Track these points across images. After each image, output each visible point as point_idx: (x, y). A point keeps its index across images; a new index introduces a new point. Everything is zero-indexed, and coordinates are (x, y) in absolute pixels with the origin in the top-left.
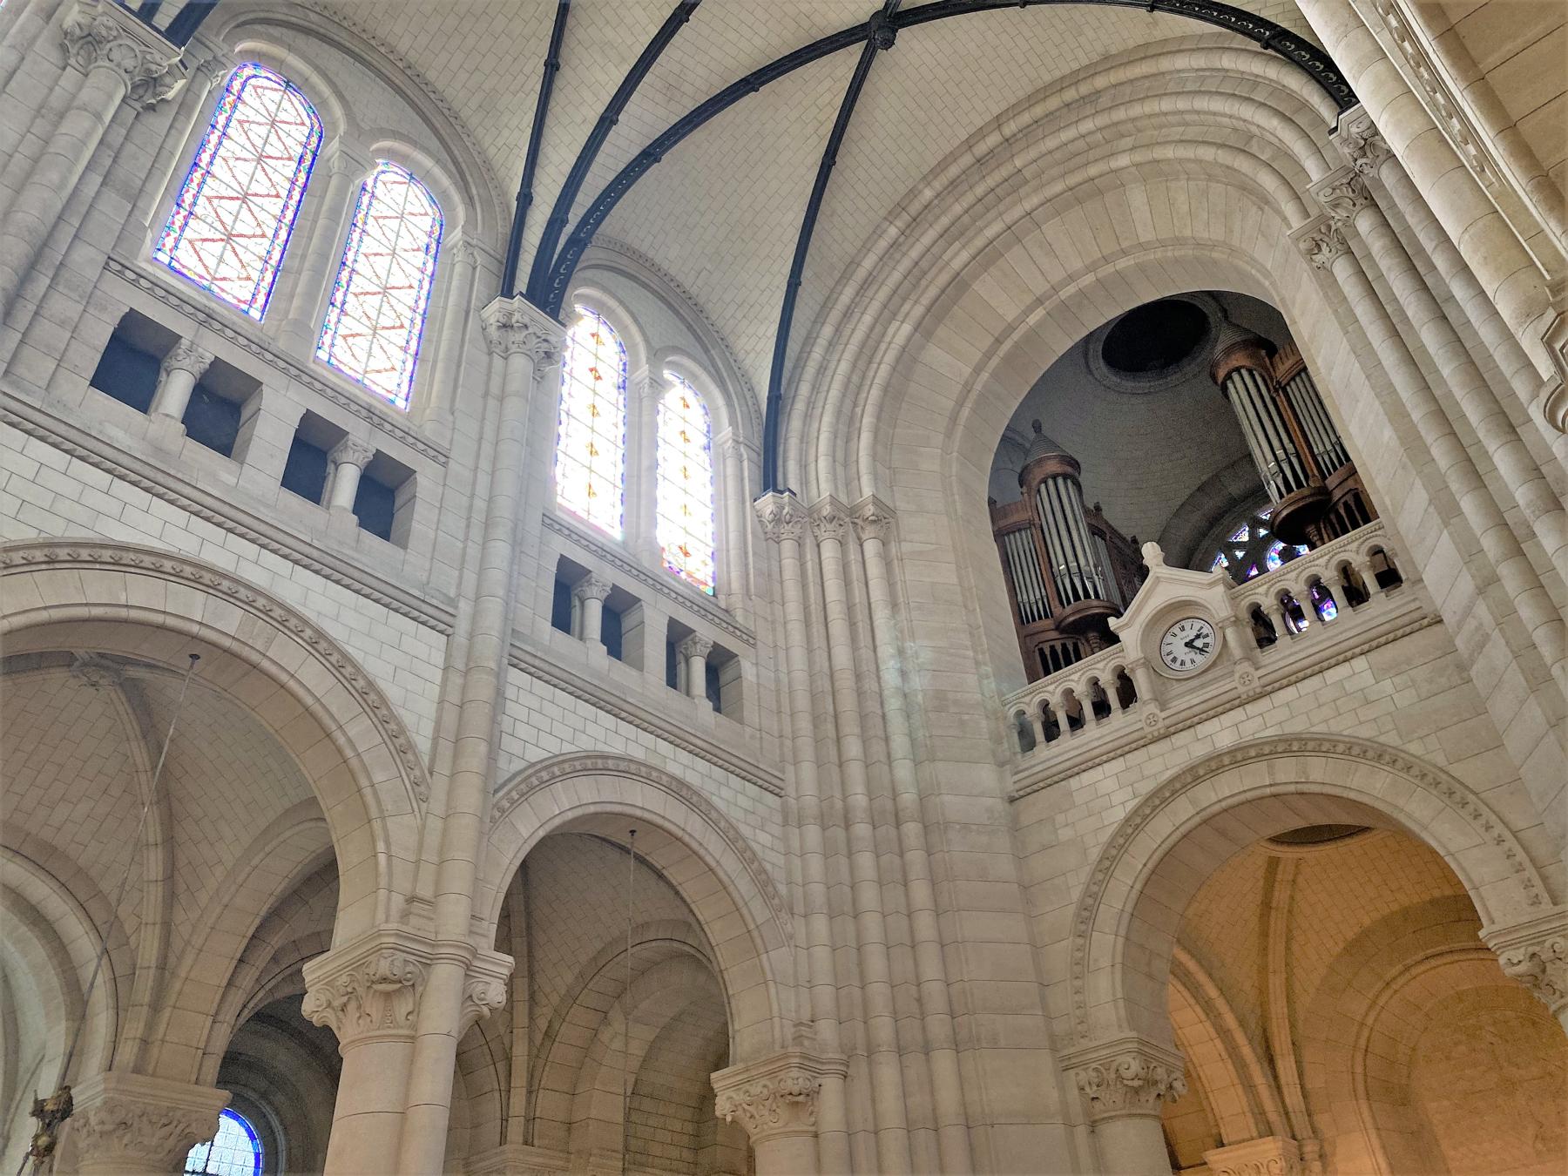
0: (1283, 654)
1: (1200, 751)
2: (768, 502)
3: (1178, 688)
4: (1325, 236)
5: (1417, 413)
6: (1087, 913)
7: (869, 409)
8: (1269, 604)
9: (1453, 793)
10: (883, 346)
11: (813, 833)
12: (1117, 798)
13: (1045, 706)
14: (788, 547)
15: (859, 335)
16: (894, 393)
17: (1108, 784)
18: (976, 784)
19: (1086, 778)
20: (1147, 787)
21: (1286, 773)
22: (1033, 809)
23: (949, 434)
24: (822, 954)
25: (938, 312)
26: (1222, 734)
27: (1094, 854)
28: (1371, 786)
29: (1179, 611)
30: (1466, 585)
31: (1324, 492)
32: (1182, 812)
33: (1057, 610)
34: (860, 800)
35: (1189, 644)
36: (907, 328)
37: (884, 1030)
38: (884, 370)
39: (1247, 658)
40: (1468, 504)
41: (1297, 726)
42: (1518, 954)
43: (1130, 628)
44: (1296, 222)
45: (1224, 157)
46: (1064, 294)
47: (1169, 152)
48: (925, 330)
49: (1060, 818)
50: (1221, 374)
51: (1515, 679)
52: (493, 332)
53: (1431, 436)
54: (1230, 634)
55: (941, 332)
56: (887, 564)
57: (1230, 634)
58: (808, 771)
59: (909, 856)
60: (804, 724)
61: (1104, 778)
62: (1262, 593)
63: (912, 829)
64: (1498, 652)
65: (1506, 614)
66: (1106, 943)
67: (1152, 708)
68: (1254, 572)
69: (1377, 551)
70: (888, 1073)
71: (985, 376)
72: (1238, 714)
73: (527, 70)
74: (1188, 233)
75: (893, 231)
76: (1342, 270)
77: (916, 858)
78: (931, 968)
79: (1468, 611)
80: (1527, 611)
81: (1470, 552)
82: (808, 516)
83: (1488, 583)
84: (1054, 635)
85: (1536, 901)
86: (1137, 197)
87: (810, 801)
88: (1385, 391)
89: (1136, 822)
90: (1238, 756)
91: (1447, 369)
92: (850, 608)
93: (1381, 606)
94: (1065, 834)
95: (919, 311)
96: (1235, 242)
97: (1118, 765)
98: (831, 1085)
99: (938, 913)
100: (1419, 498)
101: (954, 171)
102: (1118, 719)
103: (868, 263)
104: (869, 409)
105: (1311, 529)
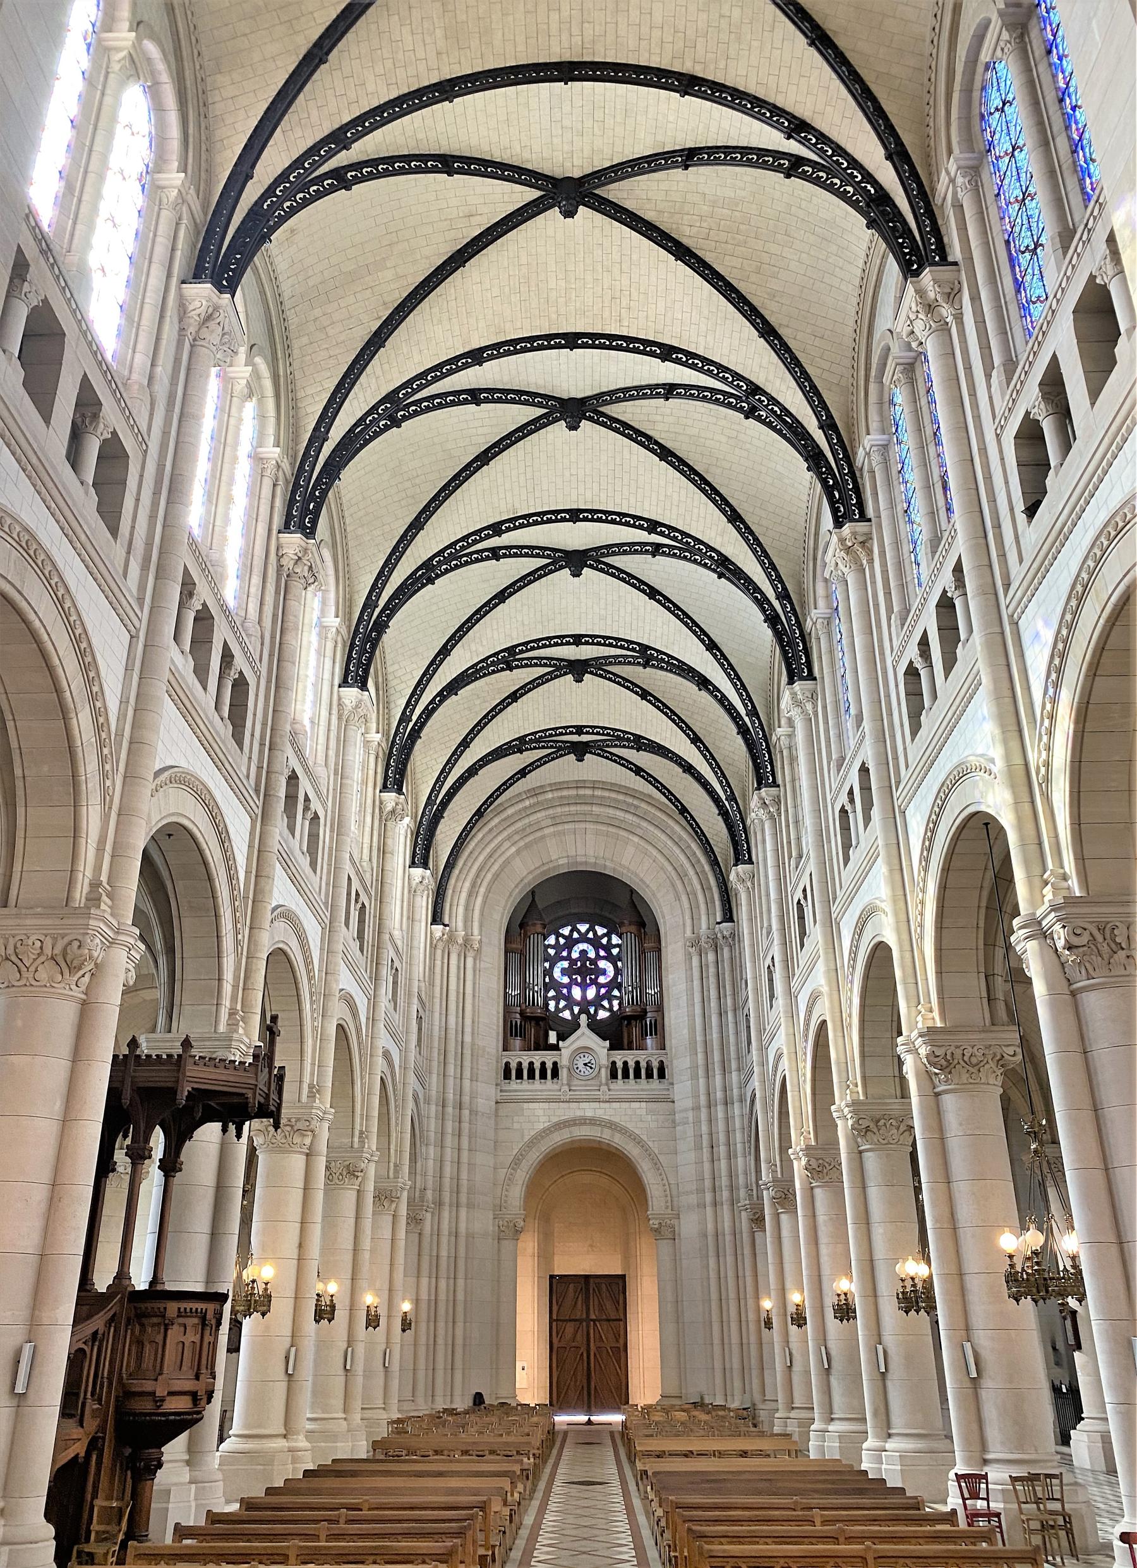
1: (579, 1113)
2: (438, 929)
3: (576, 1082)
4: (695, 943)
5: (699, 1038)
6: (516, 1162)
7: (485, 884)
8: (620, 1065)
9: (657, 1165)
10: (499, 852)
11: (433, 1108)
12: (542, 1119)
13: (520, 1064)
14: (439, 952)
15: (493, 845)
16: (496, 876)
18: (485, 1091)
19: (531, 1105)
20: (555, 1120)
21: (606, 1135)
22: (505, 1109)
23: (507, 901)
24: (431, 1163)
25: (527, 846)
26: (589, 1110)
27: (526, 1138)
28: (632, 1151)
29: (586, 1050)
30: (689, 1103)
31: (645, 1012)
33: (524, 1007)
34: (450, 1096)
35: (585, 1064)
36: (513, 849)
37: (446, 1198)
38: (496, 867)
39: (607, 1084)
40: (702, 1081)
41: (616, 1119)
42: (657, 1222)
44: (689, 933)
45: (673, 873)
46: (579, 859)
47: (655, 852)
48: (518, 852)
49: (516, 1119)
50: (624, 929)
51: (690, 1141)
52: (414, 883)
53: (700, 1049)
54: (603, 1071)
55: (524, 853)
56: (474, 971)
57: (603, 1071)
58: (434, 1077)
59: (463, 1124)
60: (436, 1055)
62: (619, 1057)
63: (466, 1113)
64: (690, 1132)
65: (697, 1122)
66: (522, 1176)
67: (566, 1088)
68: (565, 954)
69: (661, 1063)
70: (446, 1214)
71: (531, 877)
72: (596, 1105)
73: (453, 736)
74: (642, 875)
75: (527, 803)
77: (465, 1126)
78: (464, 1175)
79: (686, 1110)
80: (705, 1128)
82: (451, 939)
83: (697, 1108)
84: (518, 1016)
85: (667, 1208)
86: (631, 850)
87: (434, 1093)
88: (692, 1017)
90: (592, 1122)
91: (715, 1035)
92: (458, 992)
93: (655, 1083)
94: (516, 1126)
95: (522, 843)
96: (659, 895)
97: (546, 1105)
98: (429, 1215)
99: (470, 1150)
101: (565, 793)
102: (549, 1083)
103: (510, 811)
104: (485, 884)
105: (633, 1023)
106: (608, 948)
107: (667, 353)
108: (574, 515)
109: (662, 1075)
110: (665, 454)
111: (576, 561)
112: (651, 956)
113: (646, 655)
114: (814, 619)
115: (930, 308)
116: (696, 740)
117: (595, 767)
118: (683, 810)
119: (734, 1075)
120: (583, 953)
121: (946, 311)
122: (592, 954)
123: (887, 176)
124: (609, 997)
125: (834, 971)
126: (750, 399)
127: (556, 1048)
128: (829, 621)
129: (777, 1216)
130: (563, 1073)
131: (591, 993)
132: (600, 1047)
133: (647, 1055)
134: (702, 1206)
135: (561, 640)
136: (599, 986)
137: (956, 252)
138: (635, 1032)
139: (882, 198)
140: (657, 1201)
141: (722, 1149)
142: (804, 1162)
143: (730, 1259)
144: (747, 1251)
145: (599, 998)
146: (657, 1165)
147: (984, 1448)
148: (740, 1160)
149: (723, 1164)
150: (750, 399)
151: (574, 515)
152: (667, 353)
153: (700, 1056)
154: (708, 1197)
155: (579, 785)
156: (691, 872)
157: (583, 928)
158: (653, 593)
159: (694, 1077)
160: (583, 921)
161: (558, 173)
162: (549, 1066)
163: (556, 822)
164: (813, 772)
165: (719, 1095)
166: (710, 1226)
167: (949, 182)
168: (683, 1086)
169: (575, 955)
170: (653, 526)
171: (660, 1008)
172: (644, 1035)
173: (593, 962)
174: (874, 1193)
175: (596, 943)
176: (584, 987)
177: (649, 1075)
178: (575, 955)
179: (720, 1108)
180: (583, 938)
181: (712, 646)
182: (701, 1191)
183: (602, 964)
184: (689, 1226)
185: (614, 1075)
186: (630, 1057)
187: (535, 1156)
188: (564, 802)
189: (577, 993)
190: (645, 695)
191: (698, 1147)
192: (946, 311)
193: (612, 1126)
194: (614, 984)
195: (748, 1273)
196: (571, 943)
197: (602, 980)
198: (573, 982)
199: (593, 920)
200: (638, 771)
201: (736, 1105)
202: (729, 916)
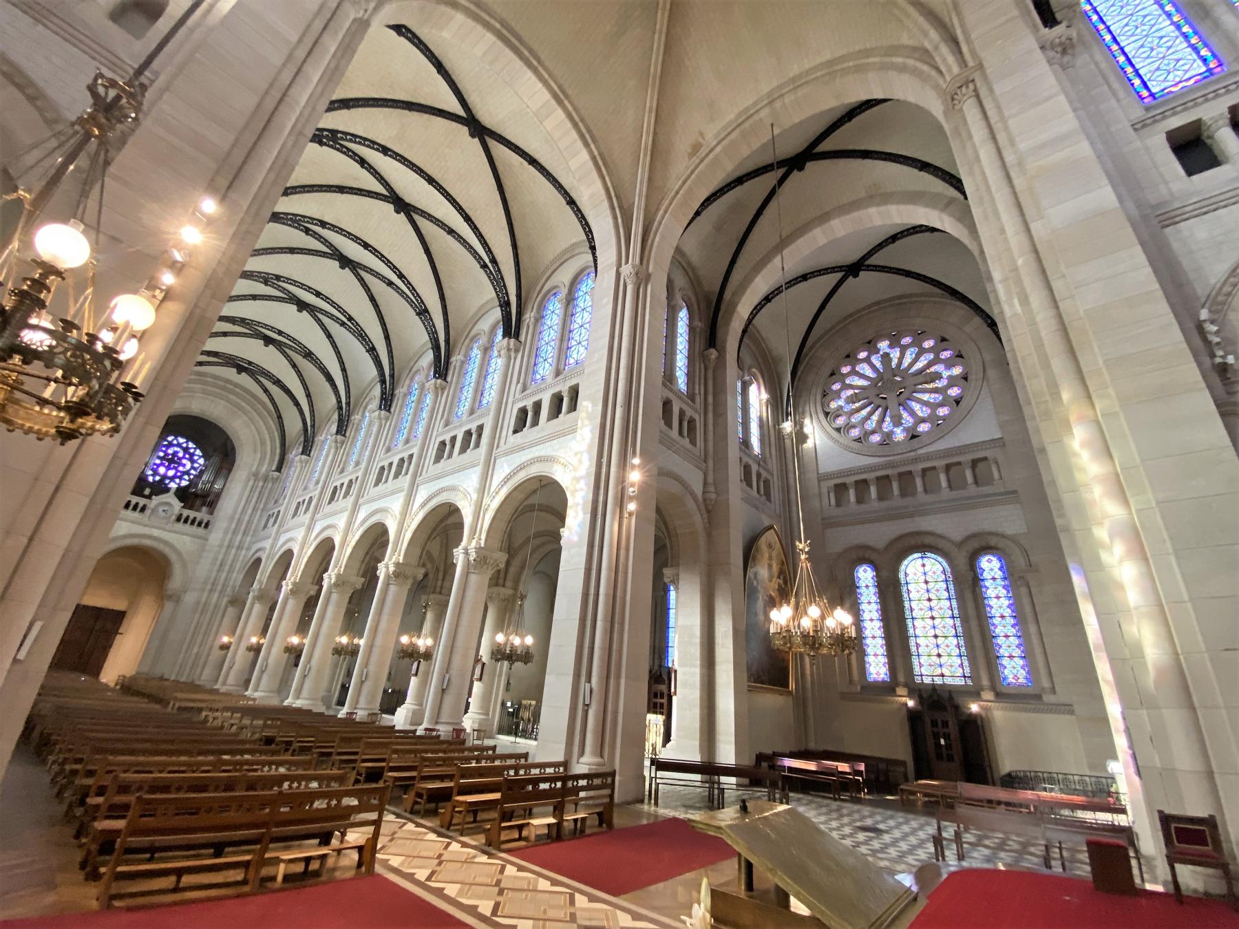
0: (180, 525)
4: (256, 475)
5: (237, 516)
17: (127, 528)
21: (161, 547)
28: (173, 557)
30: (217, 543)
32: (135, 541)
43: (156, 500)
44: (254, 468)
61: (124, 524)
62: (186, 513)
76: (251, 483)
80: (221, 557)
81: (223, 540)
83: (221, 546)
89: (125, 537)
91: (247, 518)
100: (225, 525)
106: (192, 455)
107: (401, 276)
108: (318, 294)
109: (207, 526)
110: (372, 299)
111: (302, 306)
112: (224, 471)
113: (309, 355)
114: (400, 391)
115: (509, 350)
116: (308, 396)
117: (244, 379)
118: (280, 417)
119: (249, 539)
120: (175, 453)
121: (513, 354)
122: (181, 455)
123: (513, 299)
124: (181, 478)
125: (350, 523)
126: (423, 312)
127: (149, 497)
128: (405, 395)
129: (253, 604)
130: (148, 512)
131: (171, 473)
132: (177, 505)
133: (202, 515)
134: (203, 590)
135: (272, 329)
136: (177, 471)
137: (522, 338)
138: (198, 502)
139: (508, 304)
140: (175, 582)
141: (227, 568)
142: (290, 587)
143: (208, 616)
144: (220, 614)
145: (175, 477)
146: (184, 566)
147: (357, 702)
148: (235, 575)
149: (224, 575)
150: (423, 312)
151: (318, 294)
152: (401, 276)
153: (233, 526)
154: (209, 587)
155: (228, 381)
156: (269, 443)
157: (181, 440)
158: (329, 336)
159: (226, 532)
160: (182, 437)
161: (401, 195)
162: (141, 505)
163: (204, 392)
164: (374, 446)
165: (237, 543)
166: (203, 600)
167: (529, 317)
168: (216, 536)
169: (170, 451)
170: (350, 319)
171: (218, 495)
172: (203, 504)
173: (180, 459)
174: (330, 609)
175: (186, 450)
176: (168, 468)
177: (199, 525)
178: (170, 451)
179: (233, 551)
180: (179, 445)
181: (344, 370)
182: (205, 583)
183: (184, 461)
184: (189, 598)
185: (178, 519)
186: (192, 514)
187: (113, 546)
188: (214, 385)
189: (162, 470)
190: (294, 366)
191: (213, 563)
192: (513, 354)
193: (166, 543)
194: (188, 473)
195: (217, 623)
196: (170, 445)
197: (181, 468)
198: (162, 464)
199: (188, 439)
200: (266, 391)
201: (243, 552)
202: (279, 469)
